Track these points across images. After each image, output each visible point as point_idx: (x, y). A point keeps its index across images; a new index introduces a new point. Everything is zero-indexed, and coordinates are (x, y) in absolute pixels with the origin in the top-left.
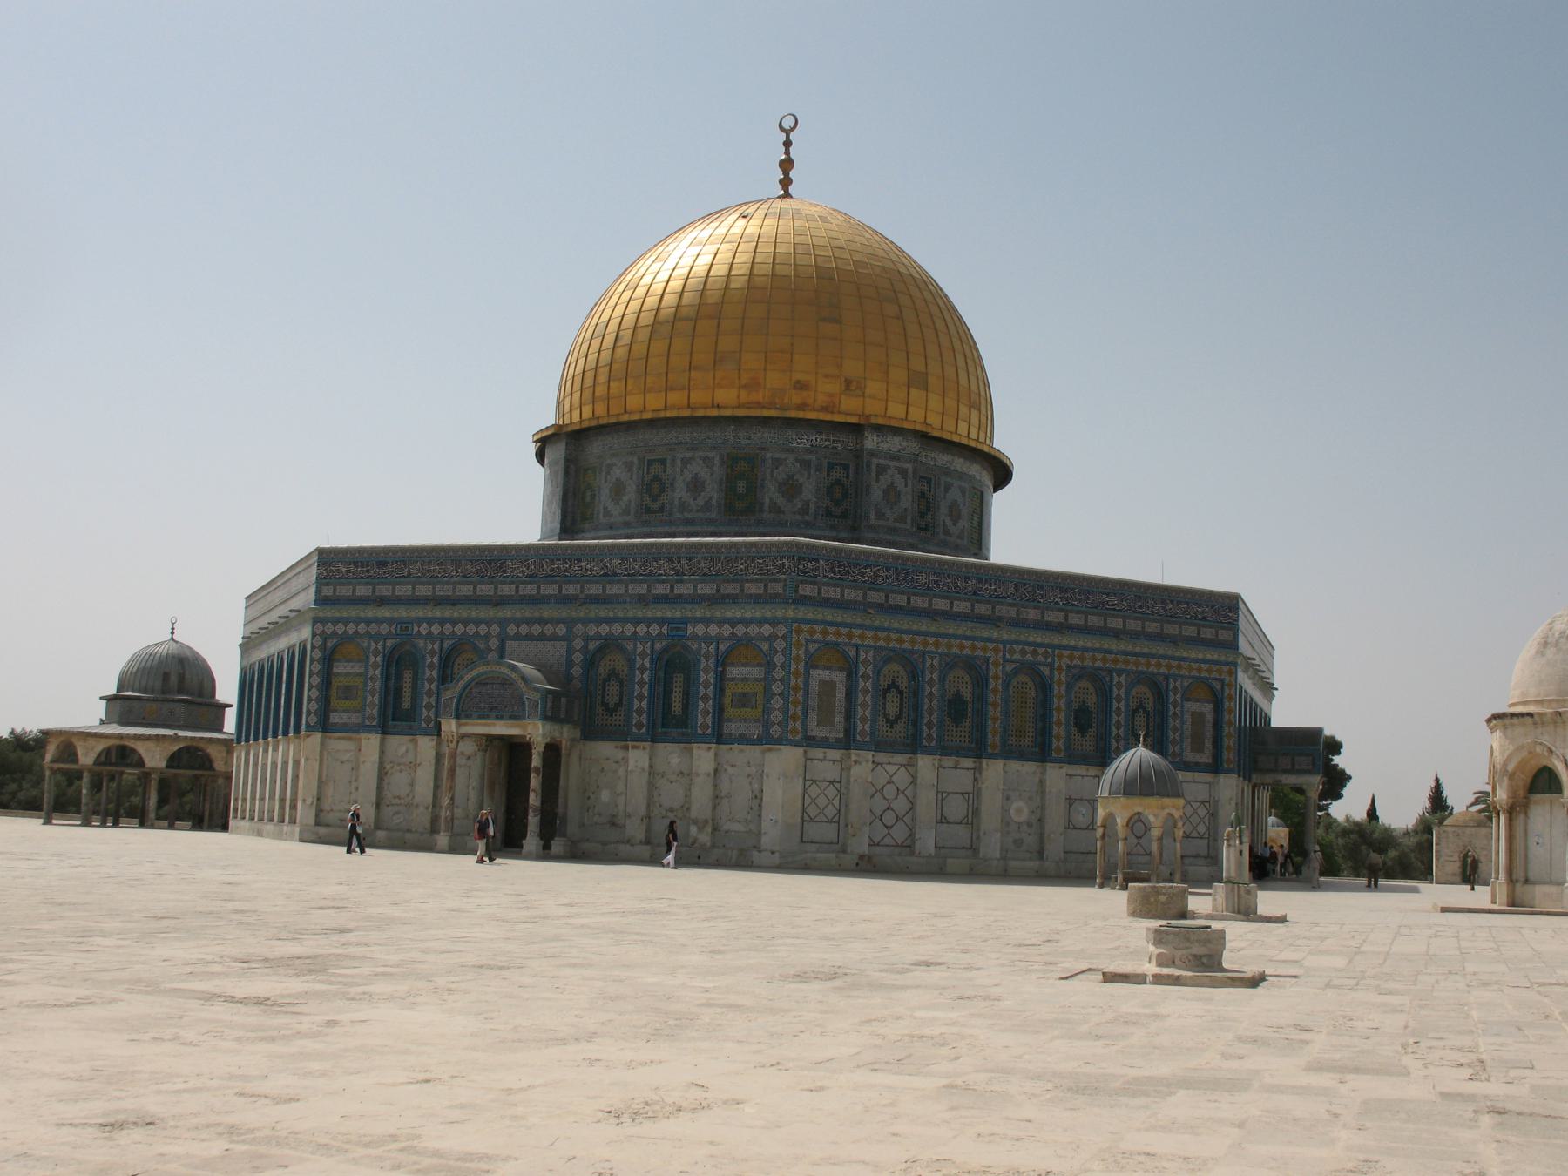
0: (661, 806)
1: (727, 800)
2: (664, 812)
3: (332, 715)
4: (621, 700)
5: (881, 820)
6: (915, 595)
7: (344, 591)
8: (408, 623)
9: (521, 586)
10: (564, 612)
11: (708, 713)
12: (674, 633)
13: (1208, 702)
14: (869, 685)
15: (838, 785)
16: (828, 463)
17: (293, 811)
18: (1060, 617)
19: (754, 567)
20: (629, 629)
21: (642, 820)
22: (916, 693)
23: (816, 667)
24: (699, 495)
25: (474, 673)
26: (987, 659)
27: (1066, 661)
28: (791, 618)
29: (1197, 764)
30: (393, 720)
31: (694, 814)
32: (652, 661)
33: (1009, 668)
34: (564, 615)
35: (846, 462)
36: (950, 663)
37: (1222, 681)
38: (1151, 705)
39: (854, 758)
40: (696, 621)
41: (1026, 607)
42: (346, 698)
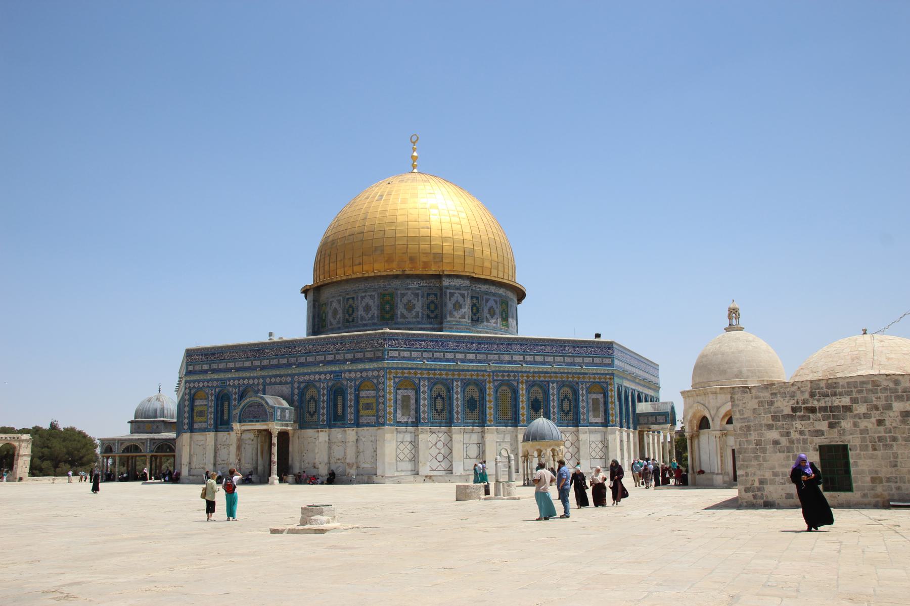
0: (334, 457)
3: (195, 424)
4: (316, 409)
5: (436, 459)
6: (447, 352)
7: (198, 368)
11: (352, 413)
12: (336, 377)
13: (601, 393)
14: (426, 396)
15: (413, 443)
16: (427, 293)
18: (521, 358)
20: (317, 377)
22: (450, 398)
23: (400, 389)
24: (369, 312)
25: (246, 402)
27: (525, 378)
28: (386, 367)
29: (596, 423)
30: (221, 425)
31: (348, 461)
32: (328, 391)
33: (496, 383)
35: (436, 293)
36: (466, 384)
37: (607, 383)
38: (571, 397)
39: (420, 430)
40: (345, 371)
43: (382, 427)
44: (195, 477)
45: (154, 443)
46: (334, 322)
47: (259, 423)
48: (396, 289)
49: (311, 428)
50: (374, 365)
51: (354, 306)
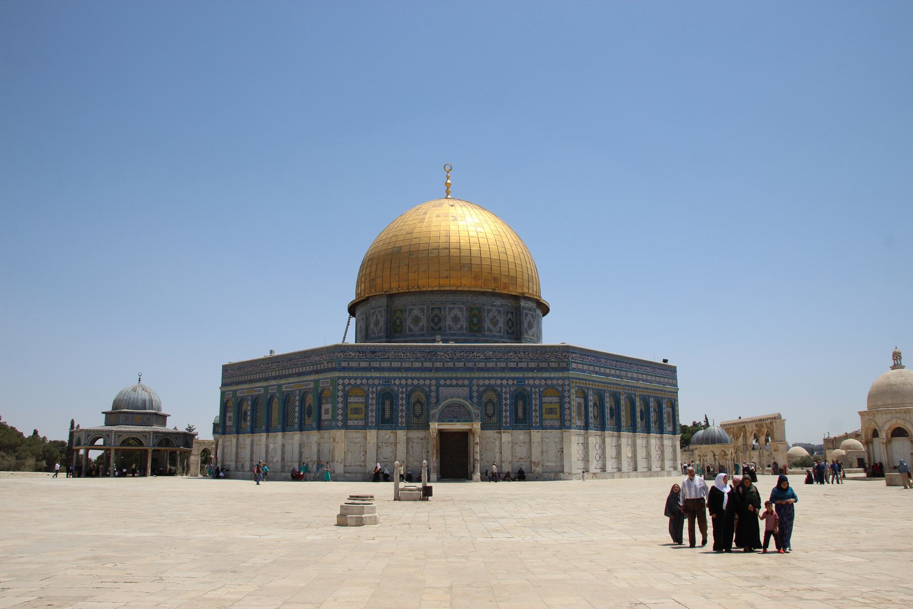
0: (516, 457)
2: (518, 459)
4: (494, 411)
7: (354, 364)
9: (445, 363)
11: (537, 417)
12: (519, 383)
16: (507, 312)
20: (499, 382)
24: (458, 323)
26: (620, 393)
30: (382, 423)
32: (510, 395)
34: (468, 376)
39: (589, 434)
40: (529, 378)
42: (356, 414)
43: (568, 430)
45: (157, 437)
46: (416, 329)
49: (490, 429)
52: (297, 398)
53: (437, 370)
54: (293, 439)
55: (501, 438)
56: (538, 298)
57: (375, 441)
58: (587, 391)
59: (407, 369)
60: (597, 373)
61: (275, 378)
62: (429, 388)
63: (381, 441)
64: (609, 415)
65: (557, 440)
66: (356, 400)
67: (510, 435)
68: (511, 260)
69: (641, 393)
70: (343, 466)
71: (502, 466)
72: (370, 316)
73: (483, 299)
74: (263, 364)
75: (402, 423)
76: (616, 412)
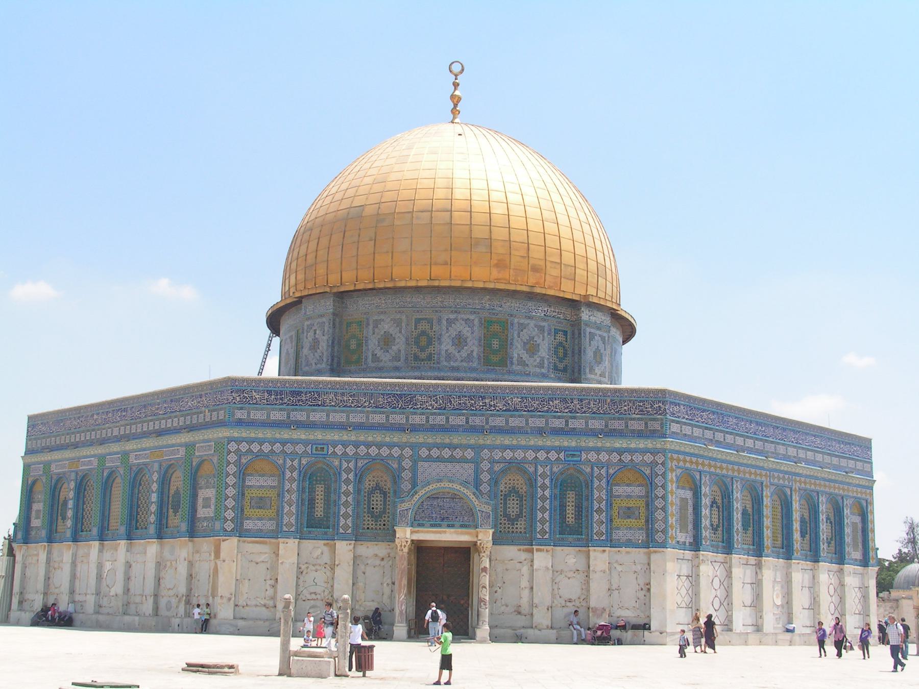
1: (618, 591)
2: (564, 602)
4: (521, 511)
7: (258, 415)
8: (323, 444)
10: (472, 440)
11: (602, 522)
12: (570, 459)
16: (555, 329)
17: (188, 606)
19: (636, 408)
20: (530, 455)
21: (548, 609)
24: (463, 348)
26: (762, 483)
34: (472, 442)
40: (589, 450)
41: (778, 444)
42: (260, 508)
43: (662, 549)
44: (251, 622)
46: (385, 358)
47: (452, 530)
48: (512, 316)
49: (512, 543)
50: (648, 444)
51: (431, 334)
52: (155, 477)
53: (414, 429)
54: (145, 553)
55: (532, 561)
56: (615, 307)
57: (294, 559)
58: (698, 477)
59: (360, 427)
60: (718, 443)
61: (119, 439)
62: (399, 463)
63: (305, 562)
64: (740, 524)
65: (638, 567)
66: (262, 481)
67: (550, 557)
68: (565, 232)
69: (803, 485)
70: (232, 606)
71: (532, 614)
72: (303, 332)
73: (510, 305)
74: (98, 414)
75: (346, 527)
76: (753, 520)
